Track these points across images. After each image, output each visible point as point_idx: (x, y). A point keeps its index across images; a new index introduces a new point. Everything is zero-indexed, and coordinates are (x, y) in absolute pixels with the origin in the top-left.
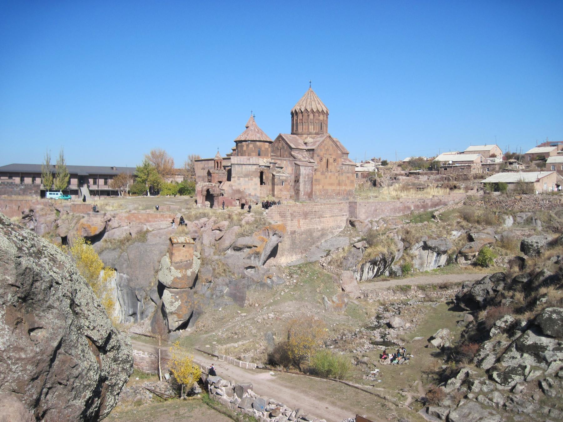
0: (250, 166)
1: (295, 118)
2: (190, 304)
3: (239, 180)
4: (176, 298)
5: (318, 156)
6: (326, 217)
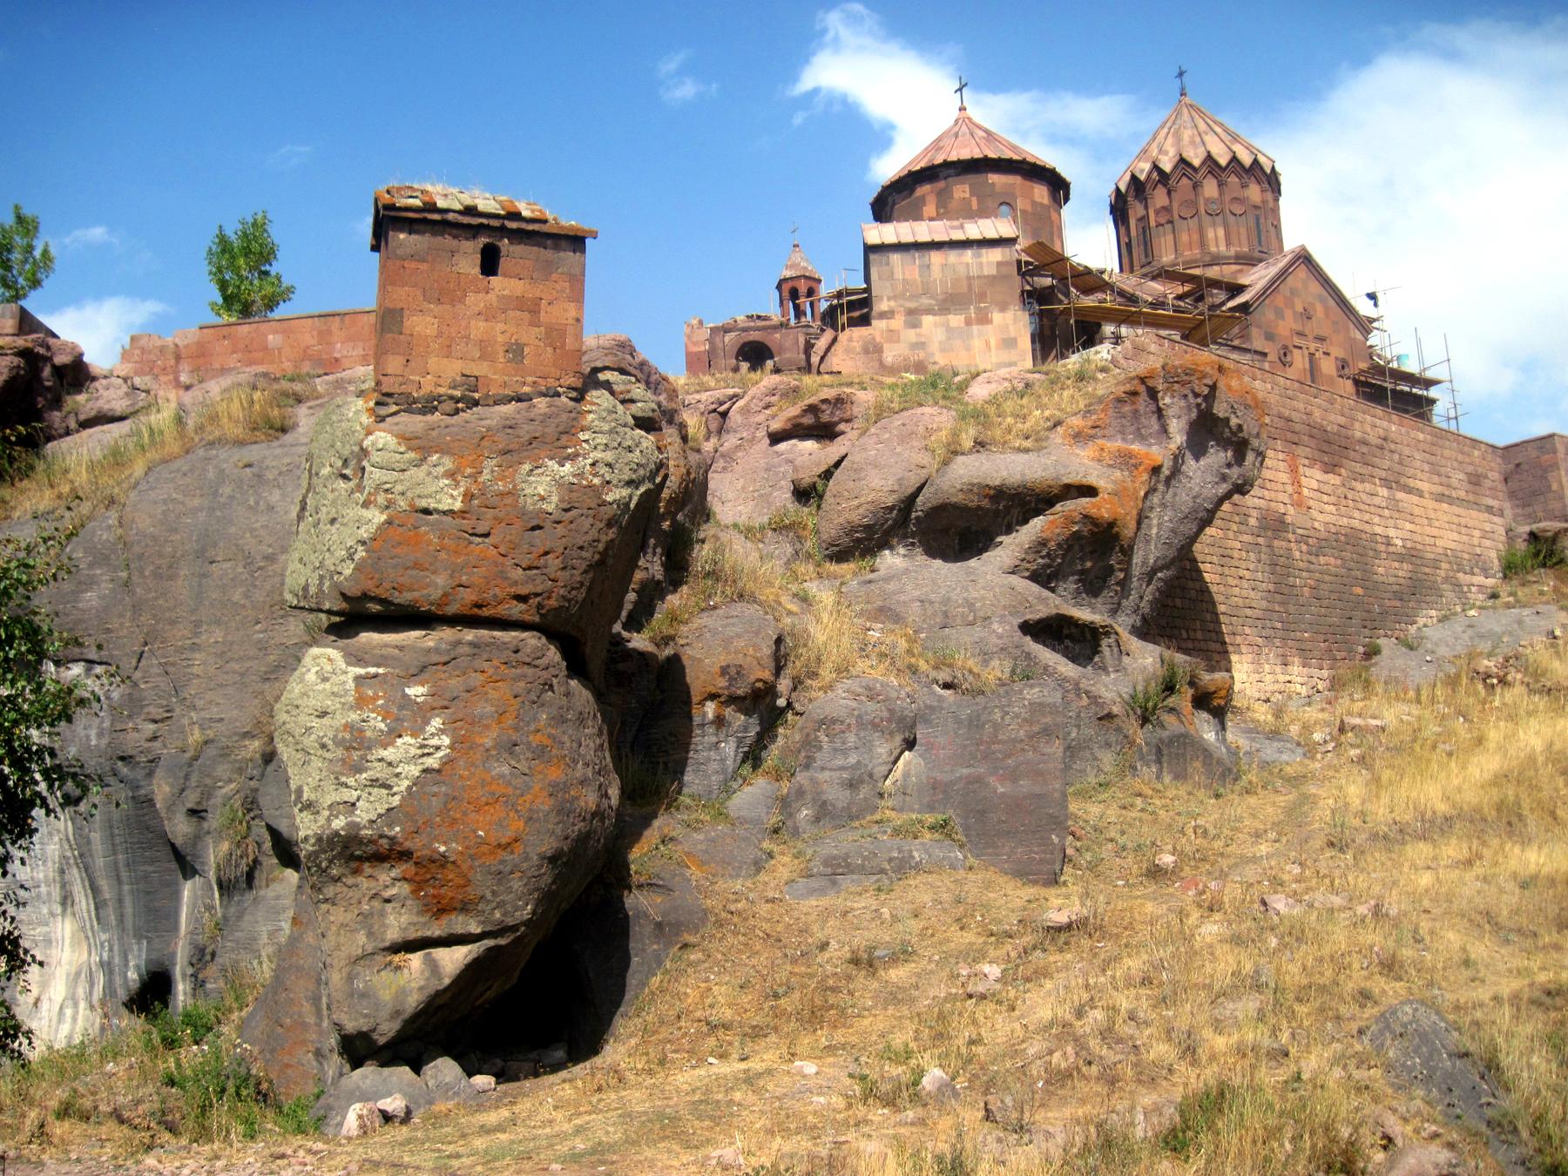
0: (969, 252)
1: (1136, 210)
3: (916, 325)
5: (1270, 337)
6: (1420, 494)
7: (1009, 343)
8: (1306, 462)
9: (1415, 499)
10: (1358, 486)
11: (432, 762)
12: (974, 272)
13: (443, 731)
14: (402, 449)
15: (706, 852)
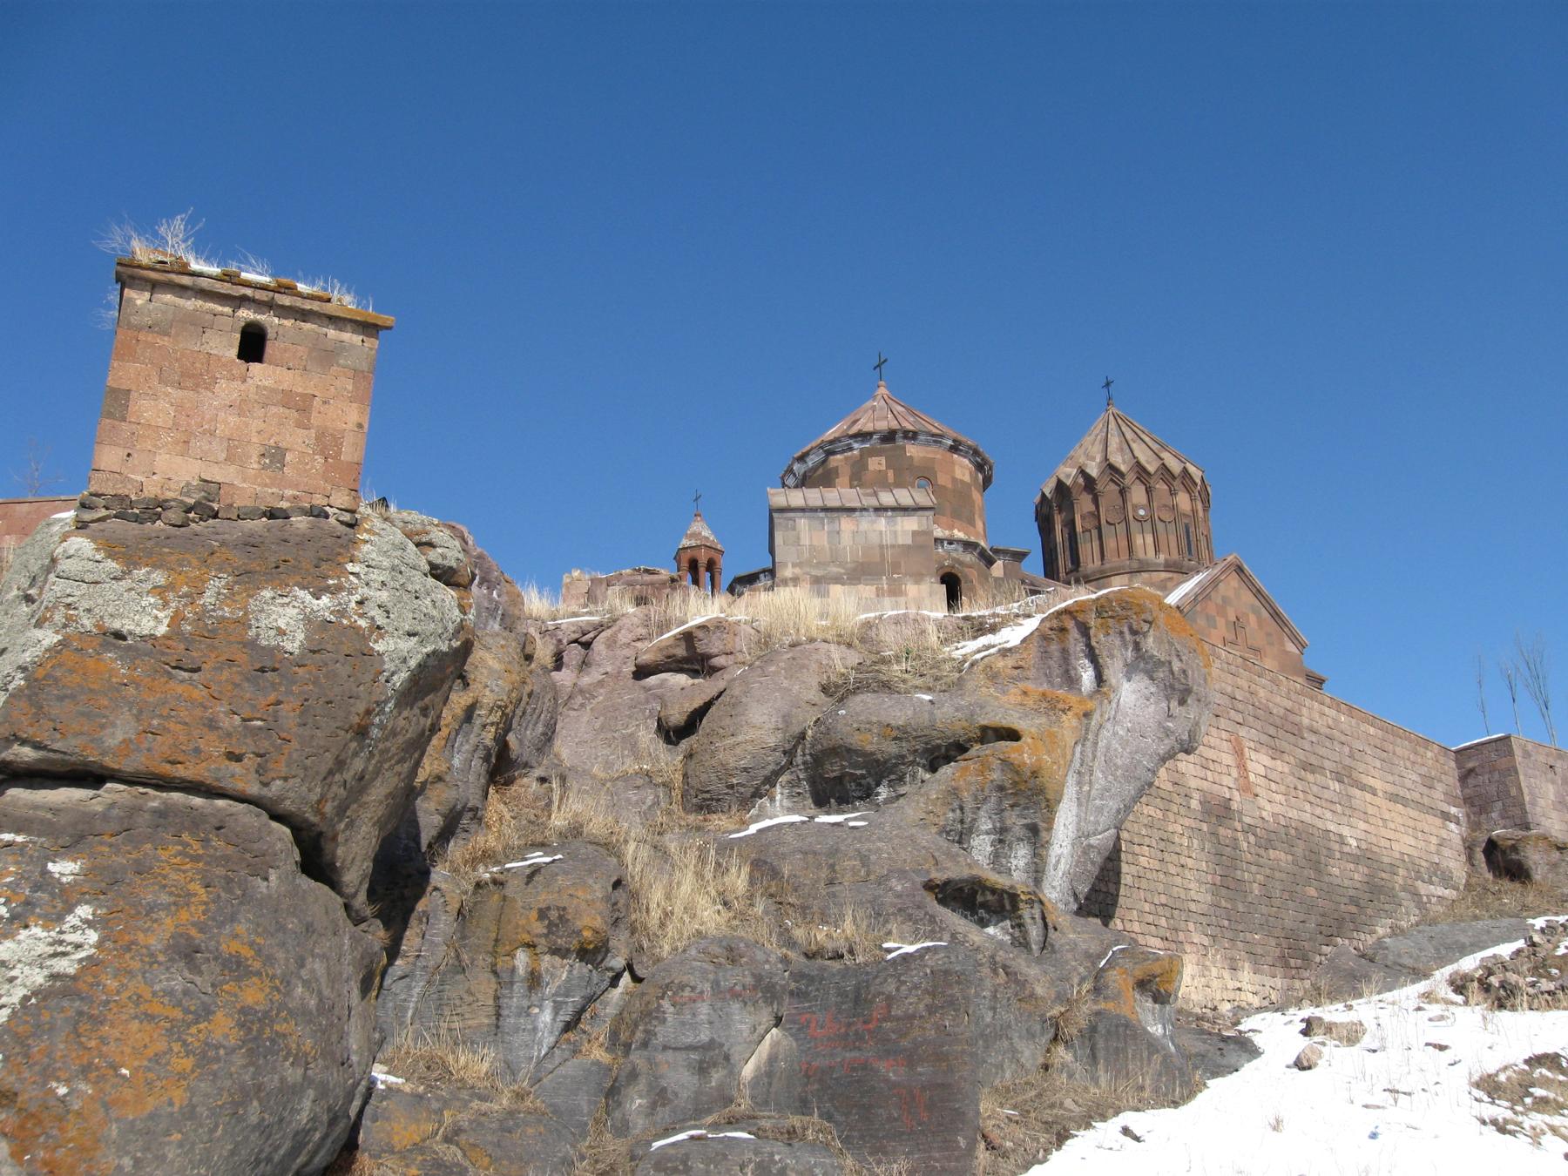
2: (253, 995)
4: (45, 882)
8: (1252, 745)
9: (1368, 797)
10: (1310, 777)
11: (66, 966)
12: (888, 540)
13: (89, 924)
14: (98, 557)
15: (499, 1145)
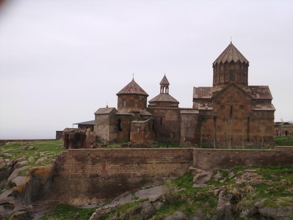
3: (98, 127)
5: (218, 103)
6: (152, 164)
7: (107, 131)
10: (126, 165)
